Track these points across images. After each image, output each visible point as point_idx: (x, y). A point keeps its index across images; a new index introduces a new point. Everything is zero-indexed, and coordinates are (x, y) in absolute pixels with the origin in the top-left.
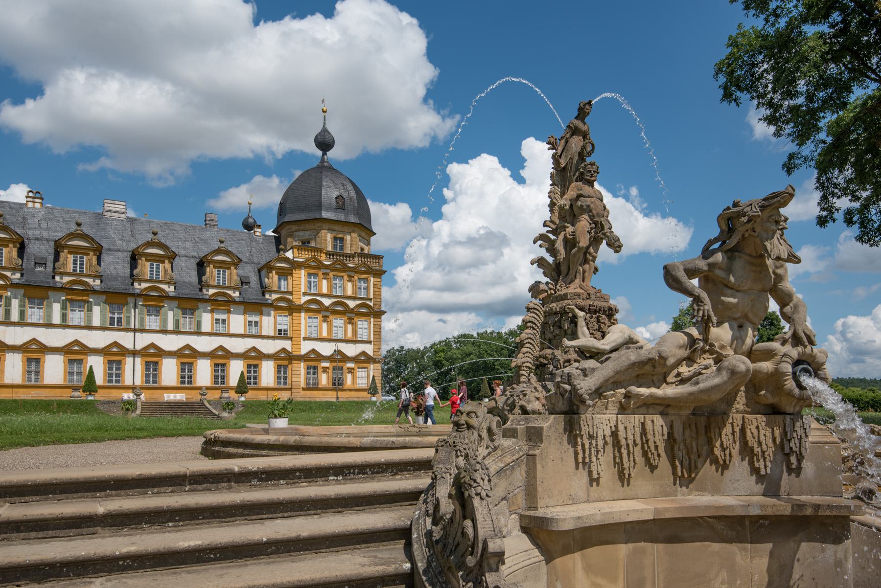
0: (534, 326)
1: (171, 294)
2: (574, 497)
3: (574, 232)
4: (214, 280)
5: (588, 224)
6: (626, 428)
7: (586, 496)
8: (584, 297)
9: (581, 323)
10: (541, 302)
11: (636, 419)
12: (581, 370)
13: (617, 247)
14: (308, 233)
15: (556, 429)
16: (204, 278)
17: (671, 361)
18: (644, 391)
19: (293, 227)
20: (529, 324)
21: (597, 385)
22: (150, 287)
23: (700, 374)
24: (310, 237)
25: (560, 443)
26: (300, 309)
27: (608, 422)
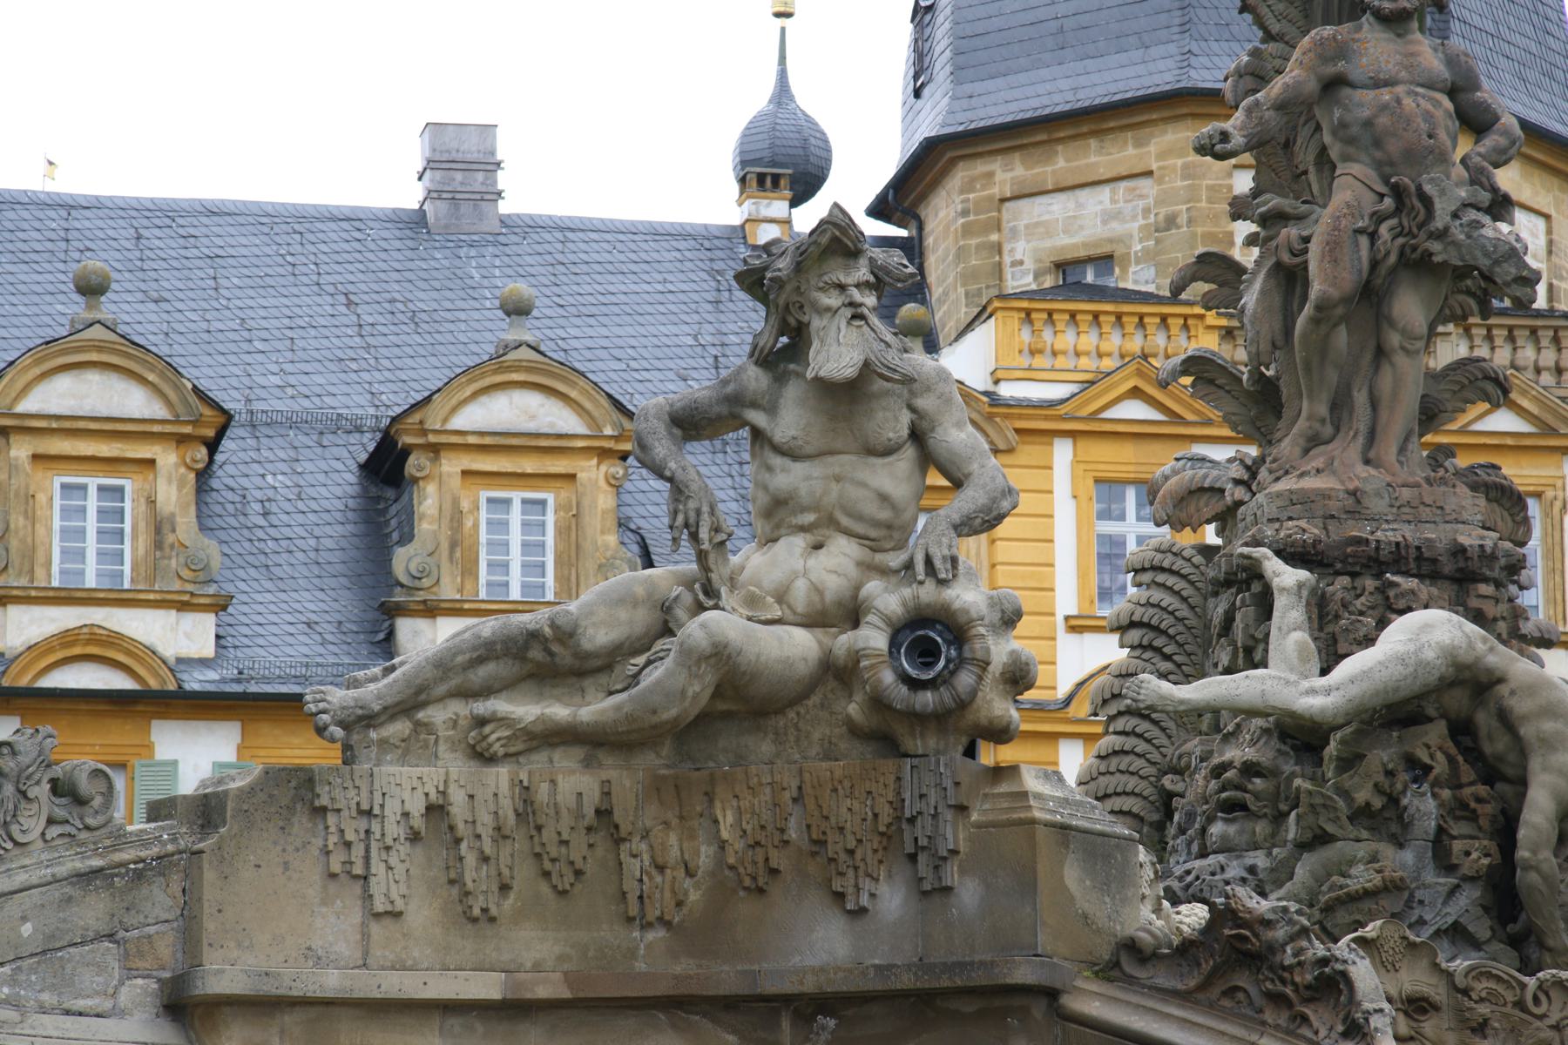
1: (196, 681)
2: (320, 952)
4: (470, 570)
5: (1371, 197)
6: (471, 797)
7: (358, 954)
8: (1334, 506)
11: (501, 776)
14: (1096, 202)
15: (271, 796)
16: (404, 560)
19: (996, 166)
22: (67, 638)
24: (1117, 228)
25: (283, 828)
26: (1054, 737)
27: (416, 783)
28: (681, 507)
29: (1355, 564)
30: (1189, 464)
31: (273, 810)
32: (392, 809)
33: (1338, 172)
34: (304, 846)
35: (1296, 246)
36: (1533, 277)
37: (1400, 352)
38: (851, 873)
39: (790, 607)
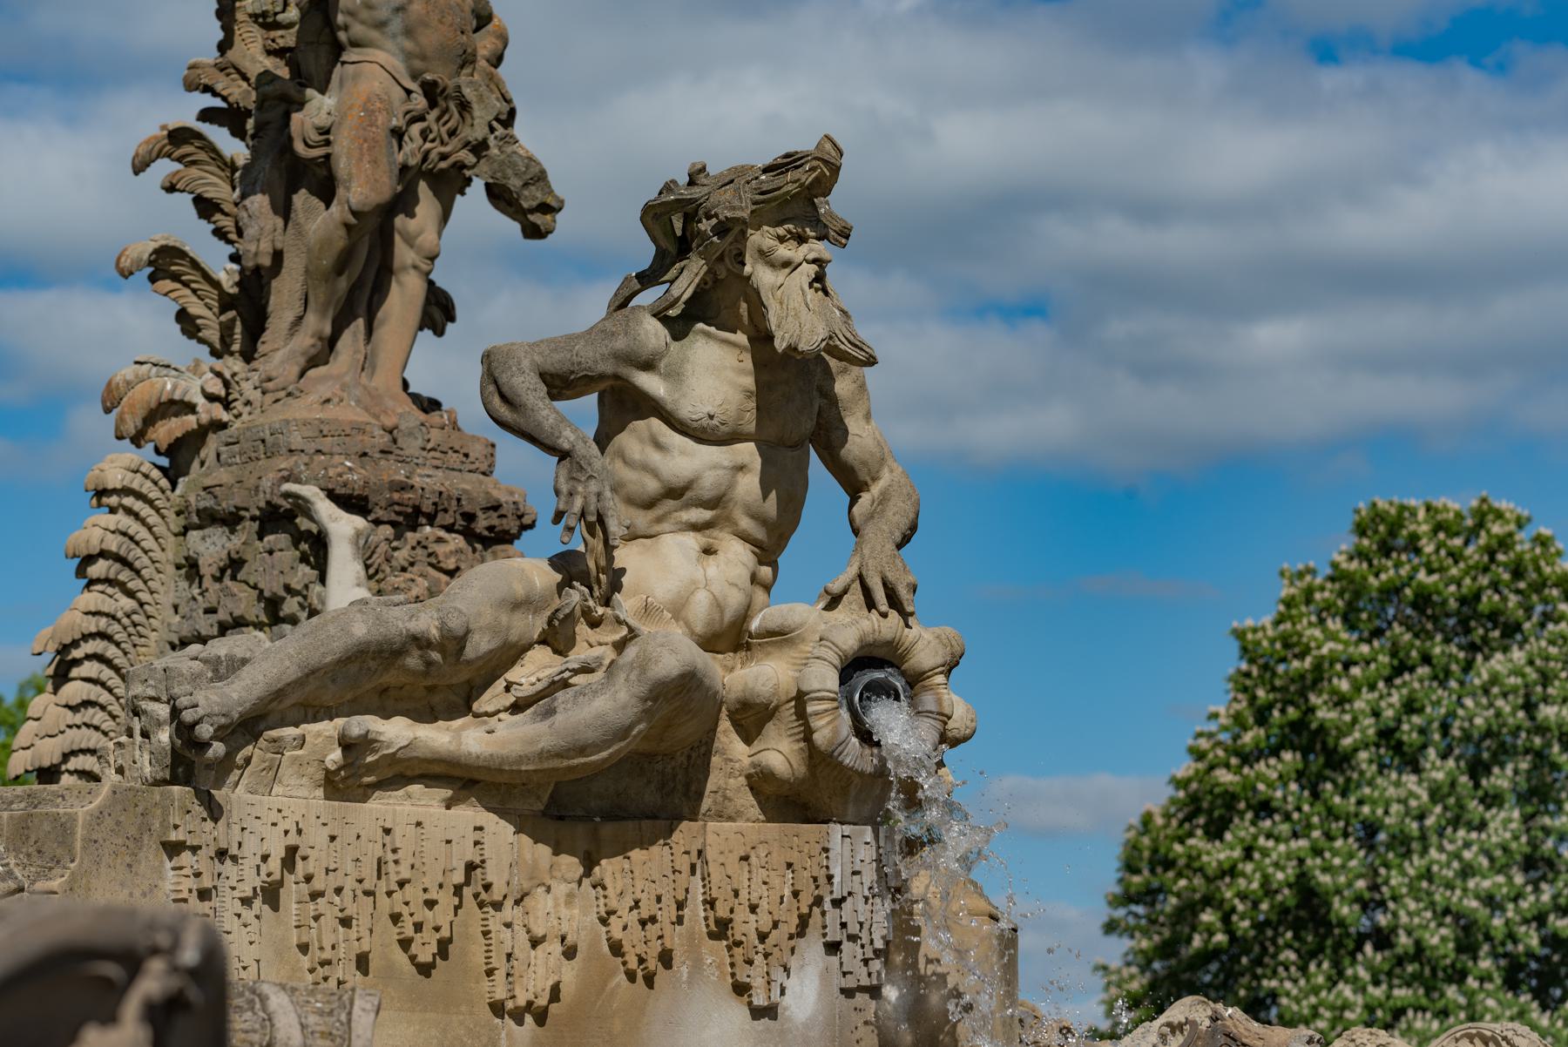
0: (125, 575)
3: (328, 132)
5: (398, 93)
6: (333, 838)
9: (344, 568)
10: (164, 462)
12: (205, 661)
13: (532, 211)
15: (118, 823)
17: (480, 644)
18: (396, 732)
20: (99, 569)
21: (248, 705)
23: (565, 684)
25: (129, 866)
28: (580, 489)
29: (398, 513)
30: (155, 369)
31: (120, 841)
32: (251, 850)
33: (344, 58)
34: (151, 891)
35: (313, 137)
36: (554, 204)
37: (412, 272)
38: (759, 959)
39: (688, 624)
